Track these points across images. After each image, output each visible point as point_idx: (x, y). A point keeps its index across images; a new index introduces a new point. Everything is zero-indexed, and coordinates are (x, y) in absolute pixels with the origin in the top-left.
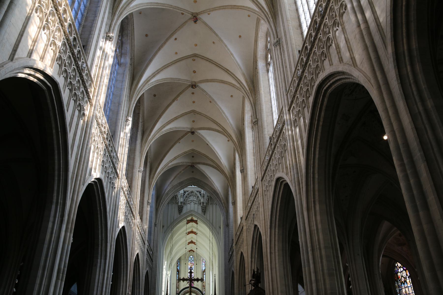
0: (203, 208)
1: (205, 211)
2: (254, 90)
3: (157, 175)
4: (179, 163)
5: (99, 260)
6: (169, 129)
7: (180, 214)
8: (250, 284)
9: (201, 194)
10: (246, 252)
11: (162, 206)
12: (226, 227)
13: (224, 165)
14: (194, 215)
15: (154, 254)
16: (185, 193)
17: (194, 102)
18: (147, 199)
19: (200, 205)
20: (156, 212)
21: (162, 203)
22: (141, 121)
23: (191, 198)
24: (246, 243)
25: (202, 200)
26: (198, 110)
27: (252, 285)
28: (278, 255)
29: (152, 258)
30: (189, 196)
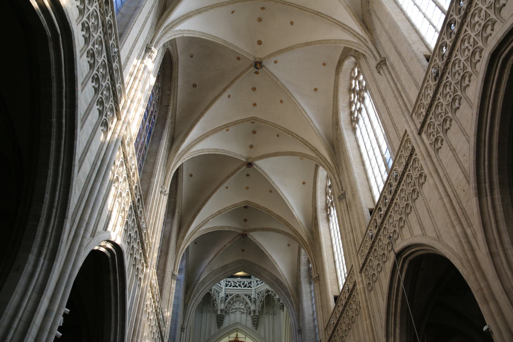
0: (254, 319)
3: (190, 234)
6: (214, 149)
7: (219, 328)
9: (250, 300)
10: (368, 331)
12: (297, 334)
13: (298, 220)
14: (241, 329)
17: (255, 105)
18: (172, 270)
19: (250, 315)
20: (184, 309)
21: (194, 296)
22: (170, 115)
23: (237, 305)
25: (253, 307)
26: (261, 116)
30: (233, 302)
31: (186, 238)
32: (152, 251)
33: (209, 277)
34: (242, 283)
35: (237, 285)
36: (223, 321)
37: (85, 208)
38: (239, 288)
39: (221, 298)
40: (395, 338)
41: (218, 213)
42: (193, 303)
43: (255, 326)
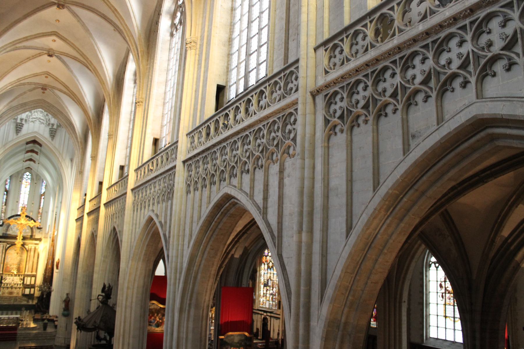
1: (54, 136)
2: (150, 31)
7: (17, 134)
8: (98, 299)
13: (88, 106)
36: (22, 128)
43: (52, 138)
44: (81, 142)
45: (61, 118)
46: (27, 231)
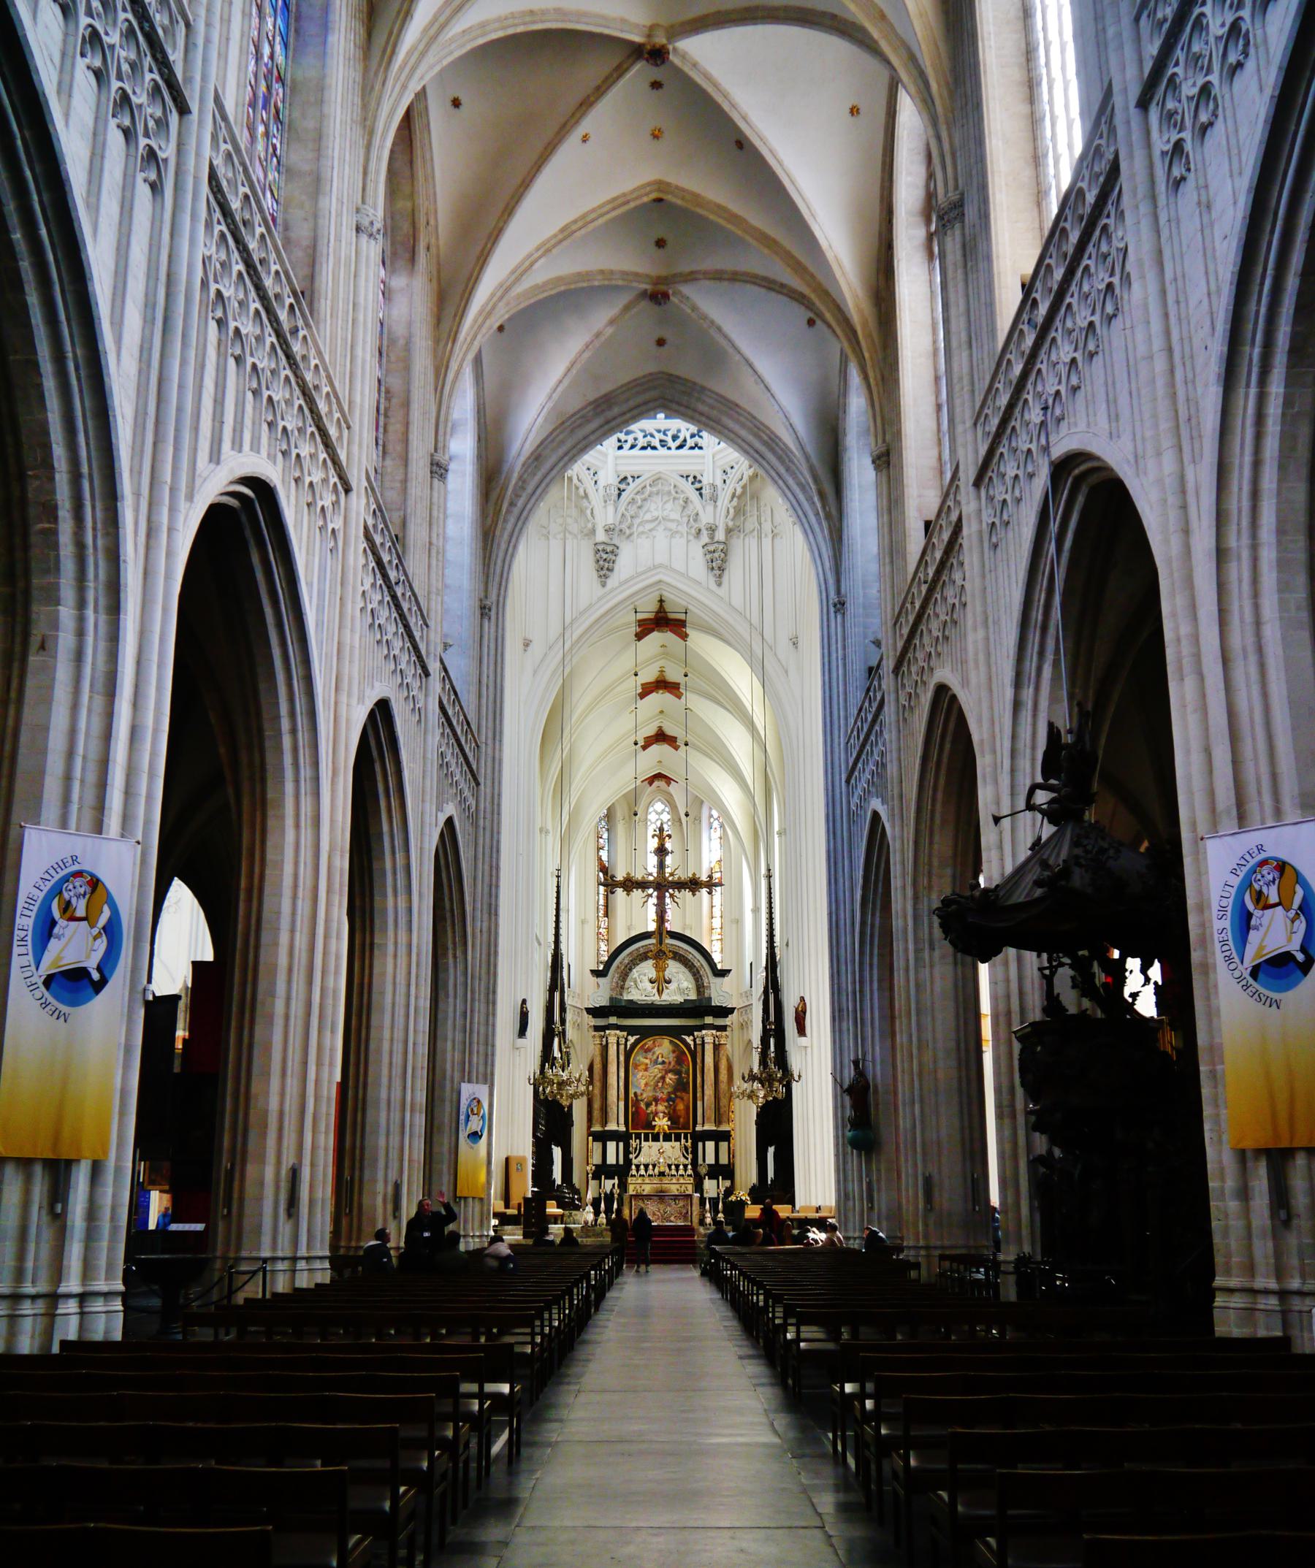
1: (721, 569)
3: (475, 321)
4: (588, 273)
5: (66, 613)
6: (523, 14)
7: (604, 585)
8: (1030, 807)
11: (512, 520)
12: (832, 615)
15: (483, 746)
16: (622, 486)
20: (485, 549)
21: (512, 504)
23: (655, 508)
24: (979, 609)
27: (1043, 813)
28: (1282, 564)
29: (474, 767)
31: (462, 336)
32: (357, 438)
33: (553, 441)
34: (670, 434)
35: (656, 443)
37: (155, 444)
38: (663, 451)
39: (605, 488)
40: (1037, 689)
41: (561, 236)
42: (509, 526)
44: (822, 495)
45: (736, 428)
46: (685, 984)
